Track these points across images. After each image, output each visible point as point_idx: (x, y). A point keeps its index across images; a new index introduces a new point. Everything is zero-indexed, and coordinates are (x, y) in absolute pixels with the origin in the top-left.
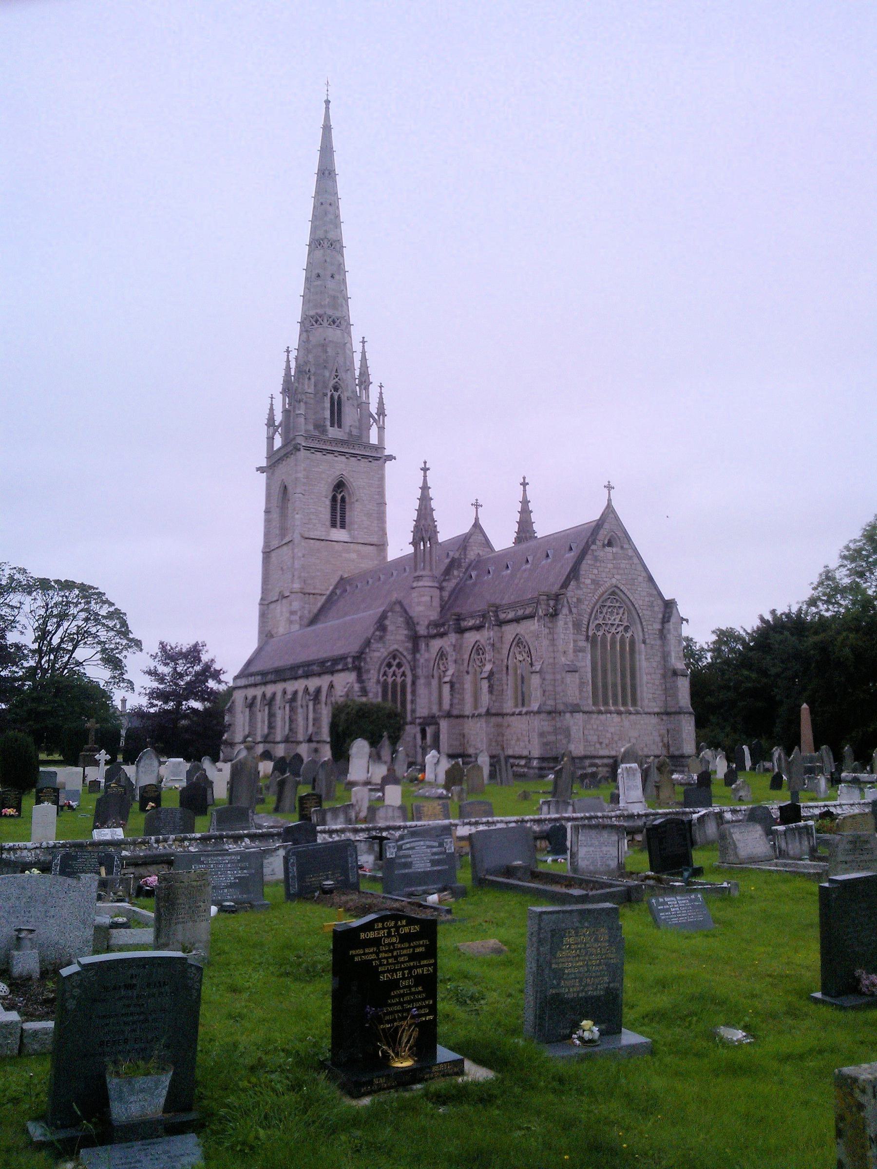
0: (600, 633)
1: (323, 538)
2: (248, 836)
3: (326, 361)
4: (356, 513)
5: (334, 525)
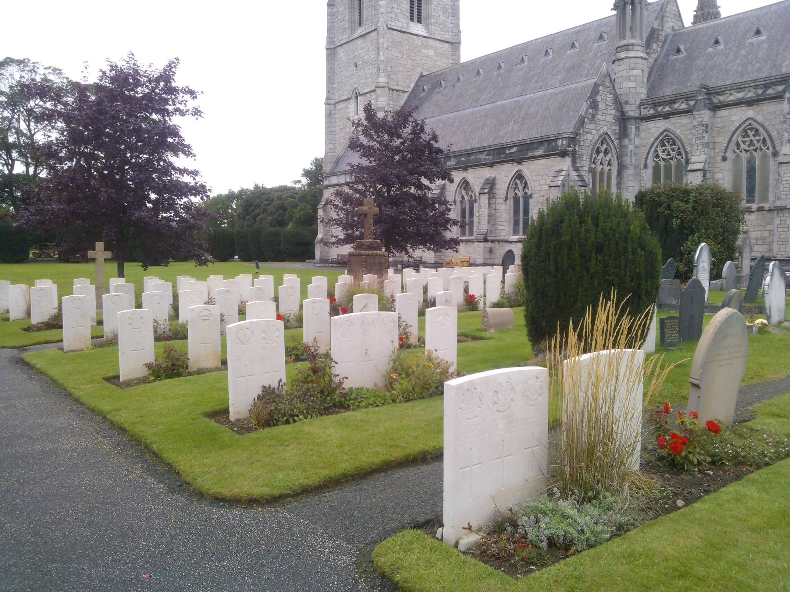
1: (404, 30)
4: (433, 6)
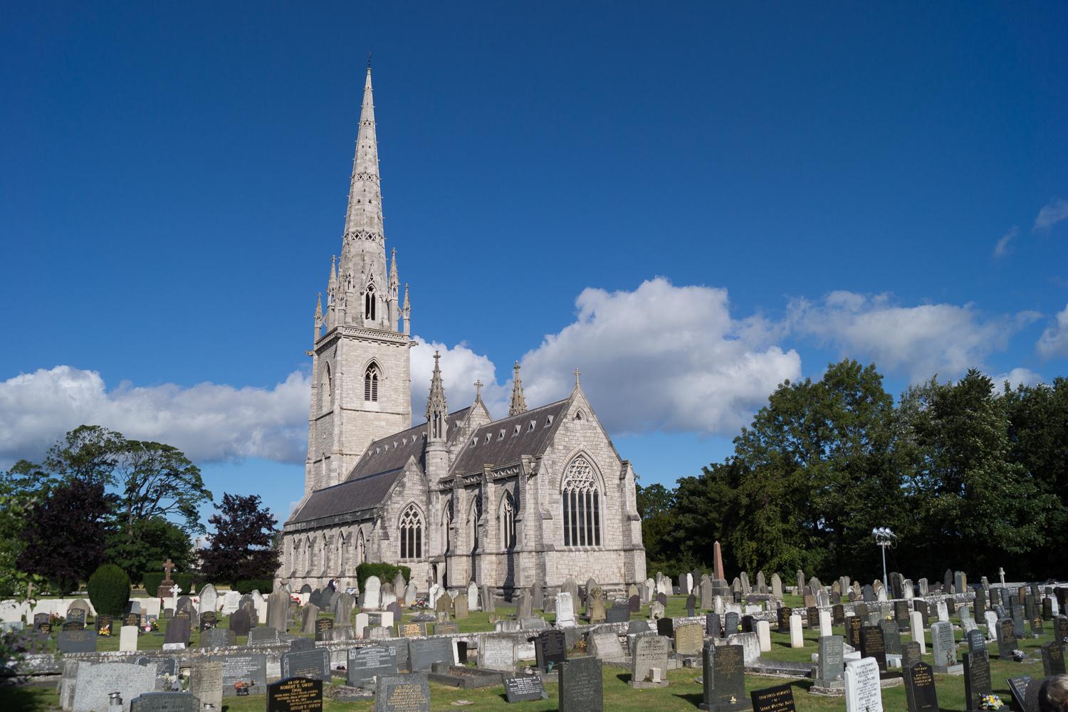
0: (571, 488)
2: (269, 647)
3: (363, 267)
5: (367, 398)
